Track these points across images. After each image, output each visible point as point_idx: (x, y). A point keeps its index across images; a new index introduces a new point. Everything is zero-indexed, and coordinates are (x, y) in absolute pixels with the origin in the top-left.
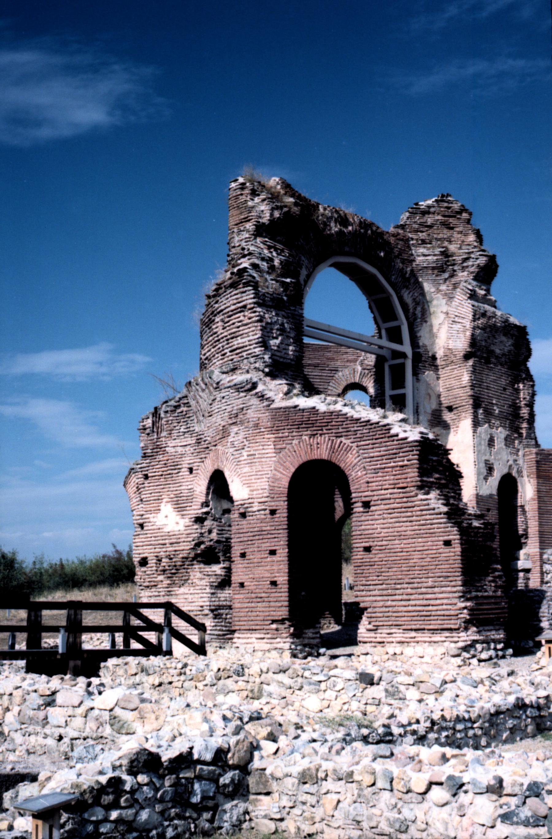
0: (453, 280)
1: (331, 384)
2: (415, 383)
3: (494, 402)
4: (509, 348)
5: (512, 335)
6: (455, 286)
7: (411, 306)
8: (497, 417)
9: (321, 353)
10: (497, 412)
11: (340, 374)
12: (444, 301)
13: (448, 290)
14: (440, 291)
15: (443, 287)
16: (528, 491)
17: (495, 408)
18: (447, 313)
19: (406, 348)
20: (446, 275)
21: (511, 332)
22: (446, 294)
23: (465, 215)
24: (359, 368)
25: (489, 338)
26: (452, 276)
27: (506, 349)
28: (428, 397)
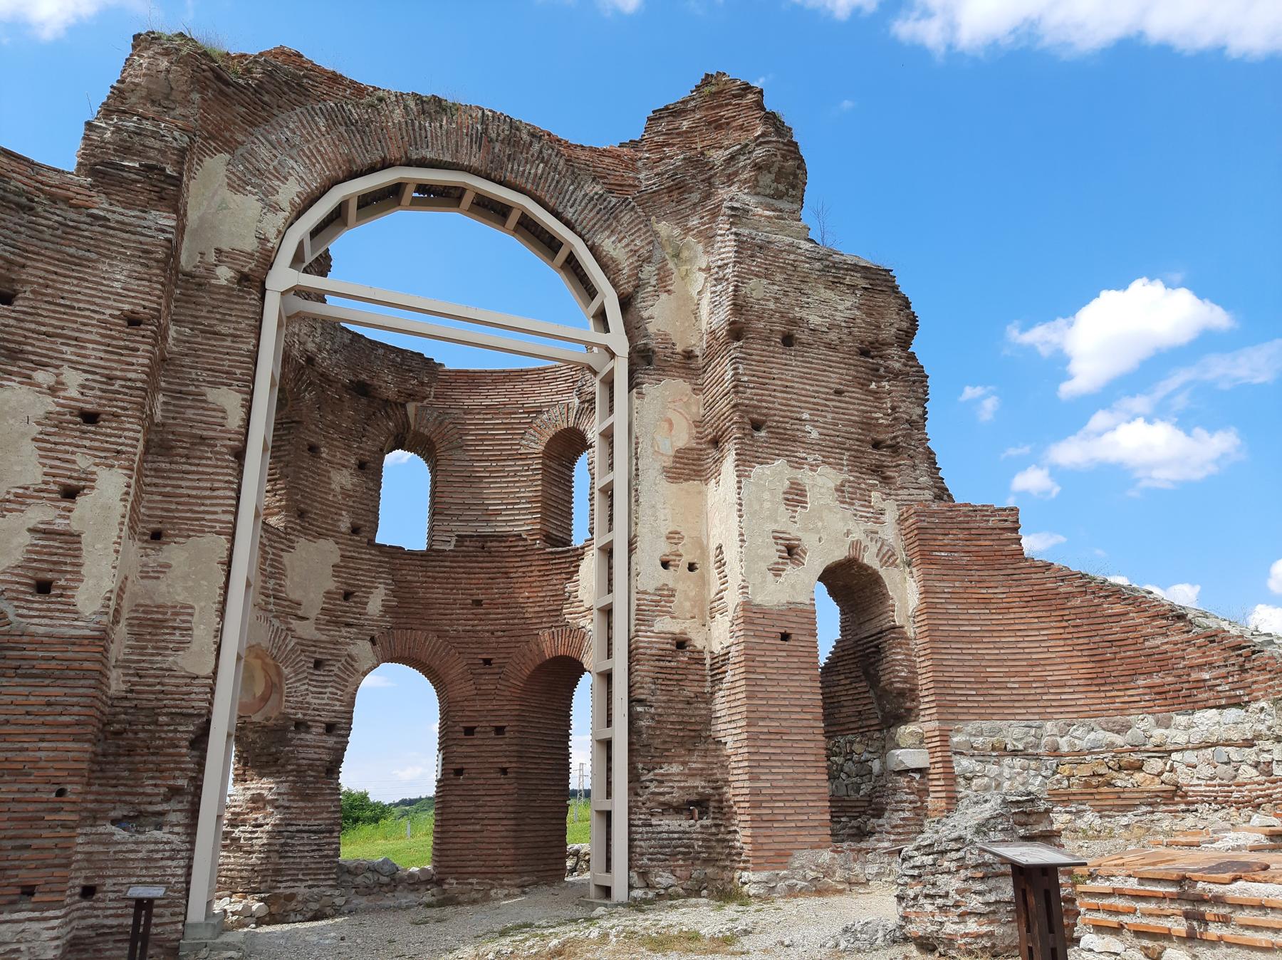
0: (710, 204)
1: (527, 436)
2: (636, 402)
3: (805, 416)
4: (848, 314)
5: (852, 287)
6: (714, 214)
7: (626, 265)
8: (811, 447)
9: (509, 386)
10: (815, 434)
11: (545, 416)
12: (700, 247)
13: (703, 224)
14: (690, 230)
15: (694, 222)
16: (905, 594)
17: (808, 428)
18: (708, 269)
19: (618, 340)
20: (695, 197)
21: (847, 281)
22: (700, 232)
23: (751, 97)
24: (577, 401)
25: (786, 294)
26: (708, 196)
27: (839, 317)
28: (666, 425)
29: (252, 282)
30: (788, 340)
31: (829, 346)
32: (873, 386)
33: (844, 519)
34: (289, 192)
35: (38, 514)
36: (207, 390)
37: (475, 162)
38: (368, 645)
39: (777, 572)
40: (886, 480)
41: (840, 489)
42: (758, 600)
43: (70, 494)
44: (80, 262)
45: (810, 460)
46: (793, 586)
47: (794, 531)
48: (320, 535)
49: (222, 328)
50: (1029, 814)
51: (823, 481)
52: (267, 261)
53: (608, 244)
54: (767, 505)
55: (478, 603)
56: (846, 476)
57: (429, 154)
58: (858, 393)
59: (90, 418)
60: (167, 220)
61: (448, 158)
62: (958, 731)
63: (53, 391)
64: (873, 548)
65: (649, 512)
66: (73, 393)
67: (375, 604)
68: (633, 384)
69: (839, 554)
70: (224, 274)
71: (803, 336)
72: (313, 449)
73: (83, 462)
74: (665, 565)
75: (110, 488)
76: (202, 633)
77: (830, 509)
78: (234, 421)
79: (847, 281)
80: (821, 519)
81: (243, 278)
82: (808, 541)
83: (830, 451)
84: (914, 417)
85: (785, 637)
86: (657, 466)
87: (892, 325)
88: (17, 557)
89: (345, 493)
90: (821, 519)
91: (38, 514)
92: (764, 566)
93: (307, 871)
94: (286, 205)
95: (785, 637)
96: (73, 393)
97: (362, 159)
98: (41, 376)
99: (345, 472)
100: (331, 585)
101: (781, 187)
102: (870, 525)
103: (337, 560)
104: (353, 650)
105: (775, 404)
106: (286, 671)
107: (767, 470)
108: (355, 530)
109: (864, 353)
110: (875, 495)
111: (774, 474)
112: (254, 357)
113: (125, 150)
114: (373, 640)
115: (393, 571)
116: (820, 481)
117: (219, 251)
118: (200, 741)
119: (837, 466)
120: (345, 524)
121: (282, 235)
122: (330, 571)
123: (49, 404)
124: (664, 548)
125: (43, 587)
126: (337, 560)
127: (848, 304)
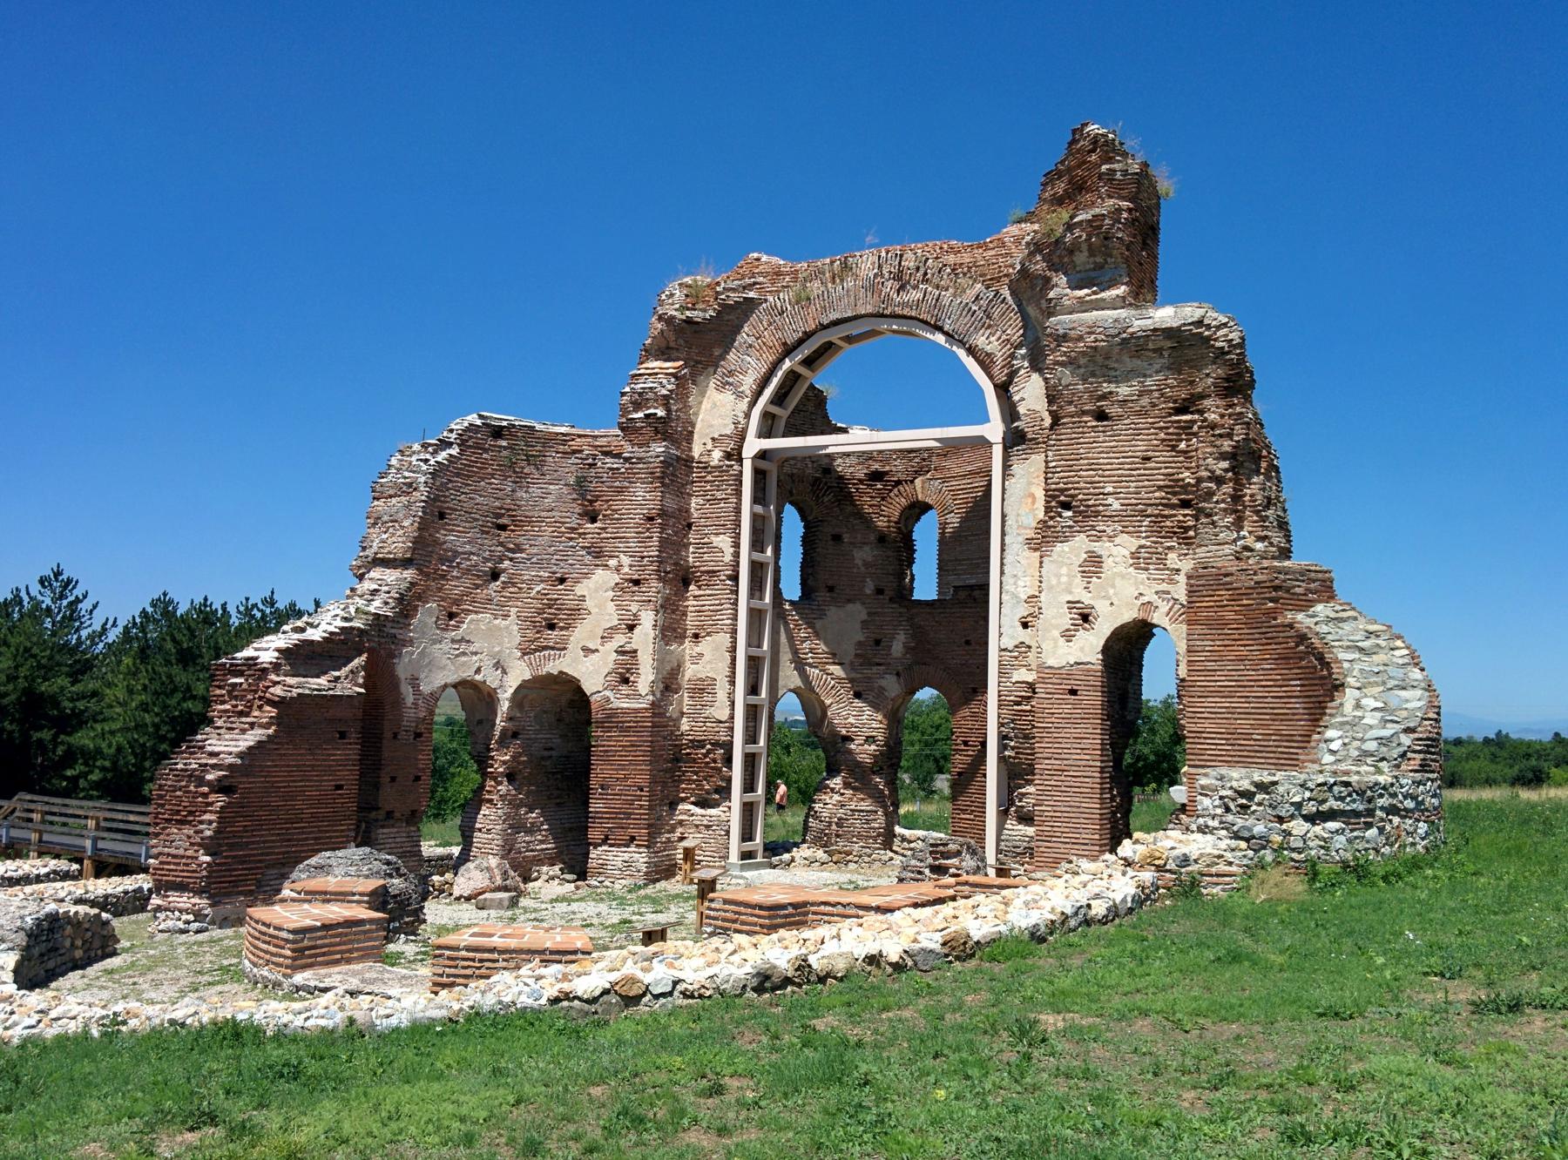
5: (1159, 351)
10: (1116, 505)
17: (1110, 500)
29: (735, 455)
30: (1101, 416)
31: (1138, 414)
32: (1183, 445)
33: (1136, 584)
34: (748, 382)
35: (620, 640)
36: (713, 538)
37: (870, 309)
38: (894, 678)
39: (1068, 636)
40: (1187, 542)
41: (1134, 555)
42: (1050, 662)
43: (631, 628)
44: (620, 490)
45: (1109, 530)
46: (1082, 649)
47: (1087, 599)
48: (849, 601)
49: (719, 495)
50: (942, 853)
51: (1118, 549)
52: (741, 437)
53: (981, 341)
54: (1064, 579)
55: (968, 643)
56: (1143, 542)
57: (834, 316)
58: (1165, 456)
59: (637, 582)
60: (658, 448)
61: (849, 314)
62: (1205, 775)
63: (618, 569)
64: (1164, 607)
65: (1011, 581)
66: (626, 570)
67: (897, 648)
68: (1006, 467)
69: (1128, 615)
70: (717, 455)
71: (1113, 410)
72: (837, 538)
73: (634, 607)
74: (1025, 625)
75: (647, 619)
76: (722, 695)
77: (1123, 576)
78: (728, 558)
79: (1151, 346)
80: (1113, 586)
81: (728, 456)
82: (1101, 607)
83: (1128, 520)
84: (1218, 472)
85: (1073, 692)
86: (1021, 539)
87: (1210, 376)
88: (611, 666)
89: (866, 564)
90: (1113, 586)
91: (620, 640)
92: (1056, 633)
93: (859, 836)
94: (748, 392)
95: (1073, 692)
96: (626, 570)
97: (792, 338)
98: (613, 562)
99: (867, 548)
100: (860, 637)
101: (1099, 260)
102: (1164, 587)
103: (864, 616)
104: (883, 683)
105: (1080, 482)
106: (828, 702)
107: (1066, 547)
108: (879, 591)
109: (1179, 411)
110: (1172, 559)
111: (1075, 548)
112: (738, 511)
113: (637, 406)
114: (898, 674)
115: (910, 619)
116: (1115, 550)
117: (713, 439)
118: (728, 761)
119: (1136, 534)
120: (869, 588)
121: (748, 416)
122: (858, 626)
123: (617, 579)
124: (1023, 611)
125: (626, 681)
126: (864, 616)
127: (1157, 367)
